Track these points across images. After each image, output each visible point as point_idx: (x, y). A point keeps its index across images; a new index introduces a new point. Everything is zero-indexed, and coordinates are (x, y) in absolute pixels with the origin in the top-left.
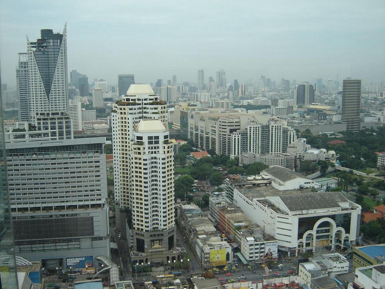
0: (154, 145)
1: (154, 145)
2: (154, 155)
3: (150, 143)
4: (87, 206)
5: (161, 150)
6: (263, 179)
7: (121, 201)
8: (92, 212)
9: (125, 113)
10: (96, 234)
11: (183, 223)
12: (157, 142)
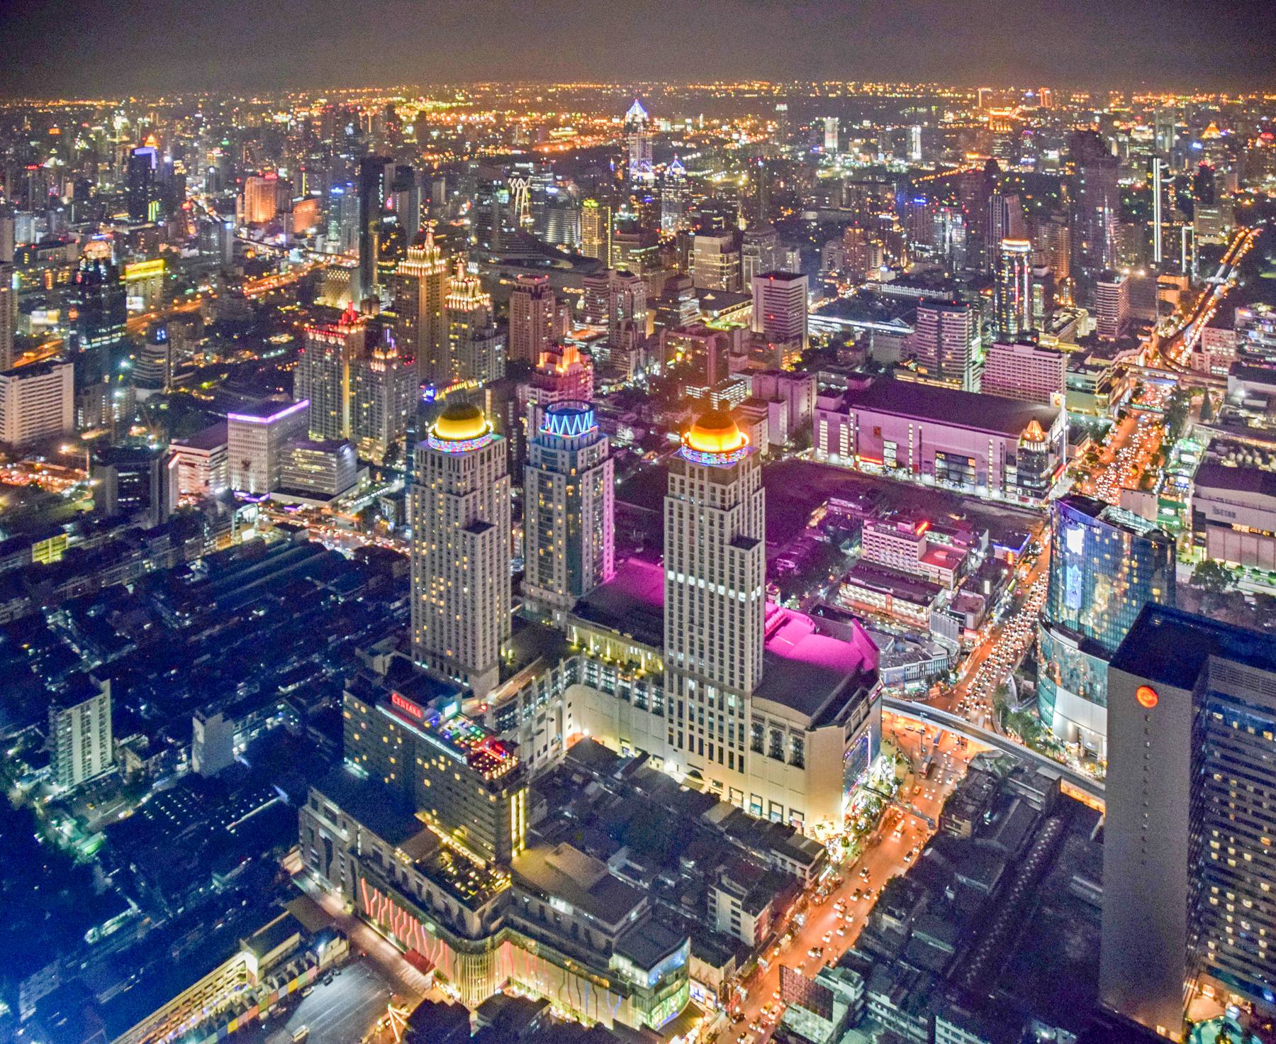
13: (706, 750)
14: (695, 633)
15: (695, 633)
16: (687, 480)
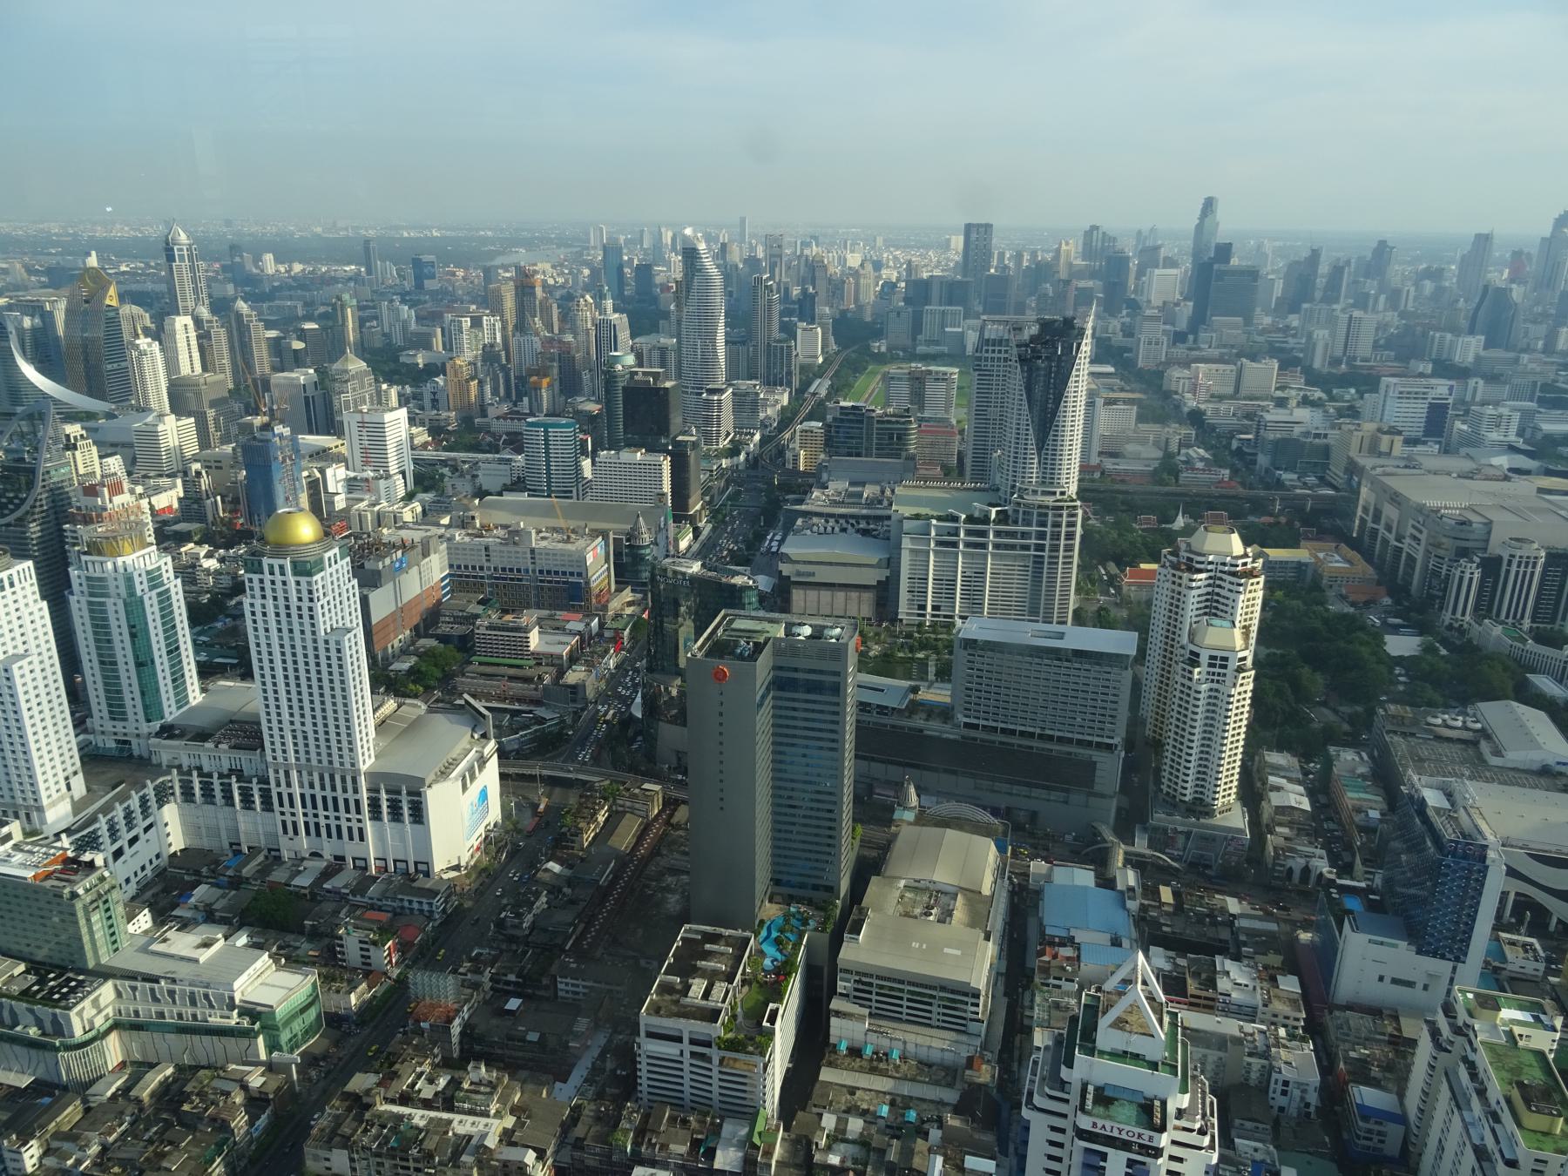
0: (1217, 670)
1: (1217, 670)
2: (1215, 686)
3: (1210, 665)
4: (1090, 744)
6: (1465, 728)
8: (1097, 756)
10: (1097, 788)
11: (1259, 784)
12: (1225, 667)
13: (323, 831)
14: (298, 726)
15: (298, 726)
16: (267, 577)
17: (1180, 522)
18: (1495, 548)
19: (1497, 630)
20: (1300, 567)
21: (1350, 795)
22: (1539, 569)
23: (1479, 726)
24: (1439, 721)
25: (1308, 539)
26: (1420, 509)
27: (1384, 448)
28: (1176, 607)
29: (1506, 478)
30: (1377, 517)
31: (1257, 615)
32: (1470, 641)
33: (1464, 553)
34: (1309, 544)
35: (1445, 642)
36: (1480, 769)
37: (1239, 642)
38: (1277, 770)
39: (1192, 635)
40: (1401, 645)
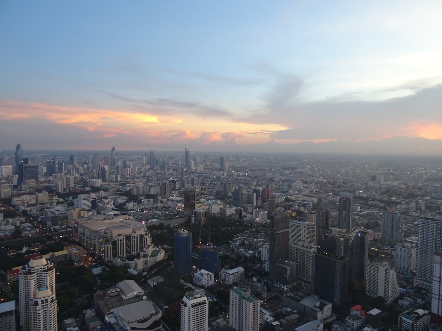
0: (45, 304)
1: (45, 304)
2: (45, 309)
3: (42, 303)
5: (49, 306)
6: (116, 291)
7: (24, 326)
9: (28, 279)
12: (47, 302)
17: (25, 249)
18: (115, 238)
19: (119, 260)
20: (65, 256)
21: (91, 324)
22: (125, 241)
23: (119, 290)
24: (110, 292)
25: (66, 246)
26: (94, 232)
27: (82, 215)
28: (27, 286)
29: (113, 218)
30: (84, 235)
31: (54, 274)
32: (113, 264)
33: (107, 241)
34: (67, 247)
35: (107, 266)
36: (122, 303)
37: (50, 293)
38: (69, 325)
39: (34, 295)
40: (97, 271)
